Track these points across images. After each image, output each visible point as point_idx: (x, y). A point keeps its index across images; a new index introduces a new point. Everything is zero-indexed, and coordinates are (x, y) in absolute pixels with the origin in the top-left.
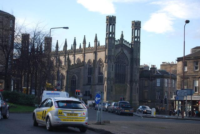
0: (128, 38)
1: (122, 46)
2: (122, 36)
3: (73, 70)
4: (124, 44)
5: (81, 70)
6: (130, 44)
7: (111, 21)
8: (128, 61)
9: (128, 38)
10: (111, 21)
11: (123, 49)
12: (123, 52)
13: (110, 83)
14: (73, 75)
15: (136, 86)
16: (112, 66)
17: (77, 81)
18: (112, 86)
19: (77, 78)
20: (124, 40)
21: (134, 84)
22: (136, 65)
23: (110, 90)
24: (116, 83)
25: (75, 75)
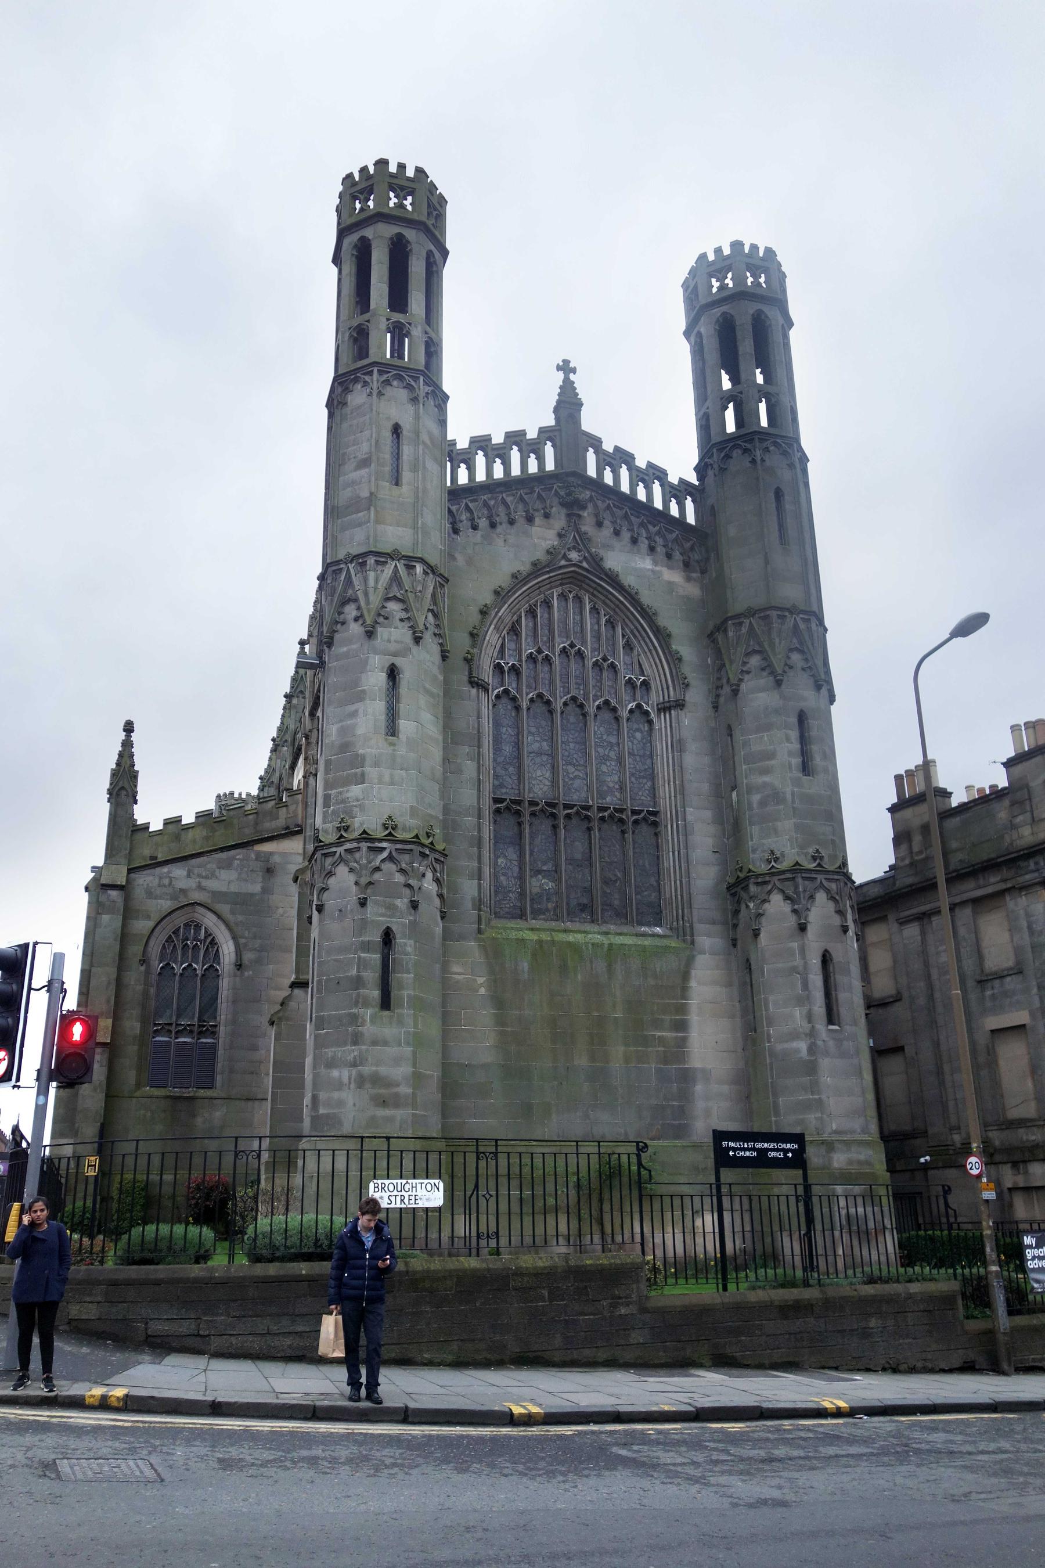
0: (655, 424)
1: (573, 507)
2: (568, 404)
3: (178, 872)
4: (597, 484)
5: (270, 871)
6: (679, 491)
7: (390, 241)
8: (675, 660)
9: (655, 424)
10: (390, 241)
11: (587, 527)
12: (596, 562)
13: (353, 894)
14: (179, 920)
15: (802, 928)
16: (393, 673)
17: (225, 984)
18: (388, 937)
19: (227, 949)
20: (596, 443)
21: (777, 905)
22: (766, 680)
23: (358, 982)
24: (522, 916)
25: (209, 921)
